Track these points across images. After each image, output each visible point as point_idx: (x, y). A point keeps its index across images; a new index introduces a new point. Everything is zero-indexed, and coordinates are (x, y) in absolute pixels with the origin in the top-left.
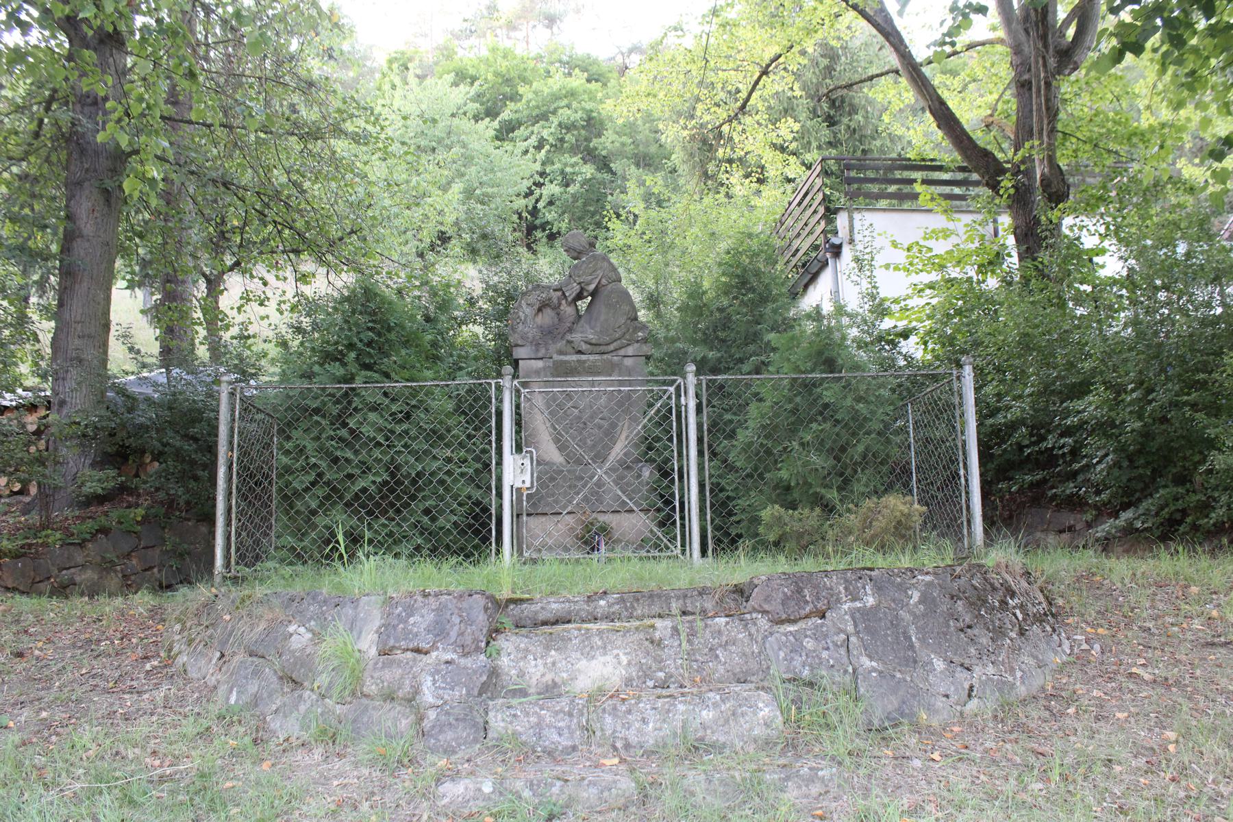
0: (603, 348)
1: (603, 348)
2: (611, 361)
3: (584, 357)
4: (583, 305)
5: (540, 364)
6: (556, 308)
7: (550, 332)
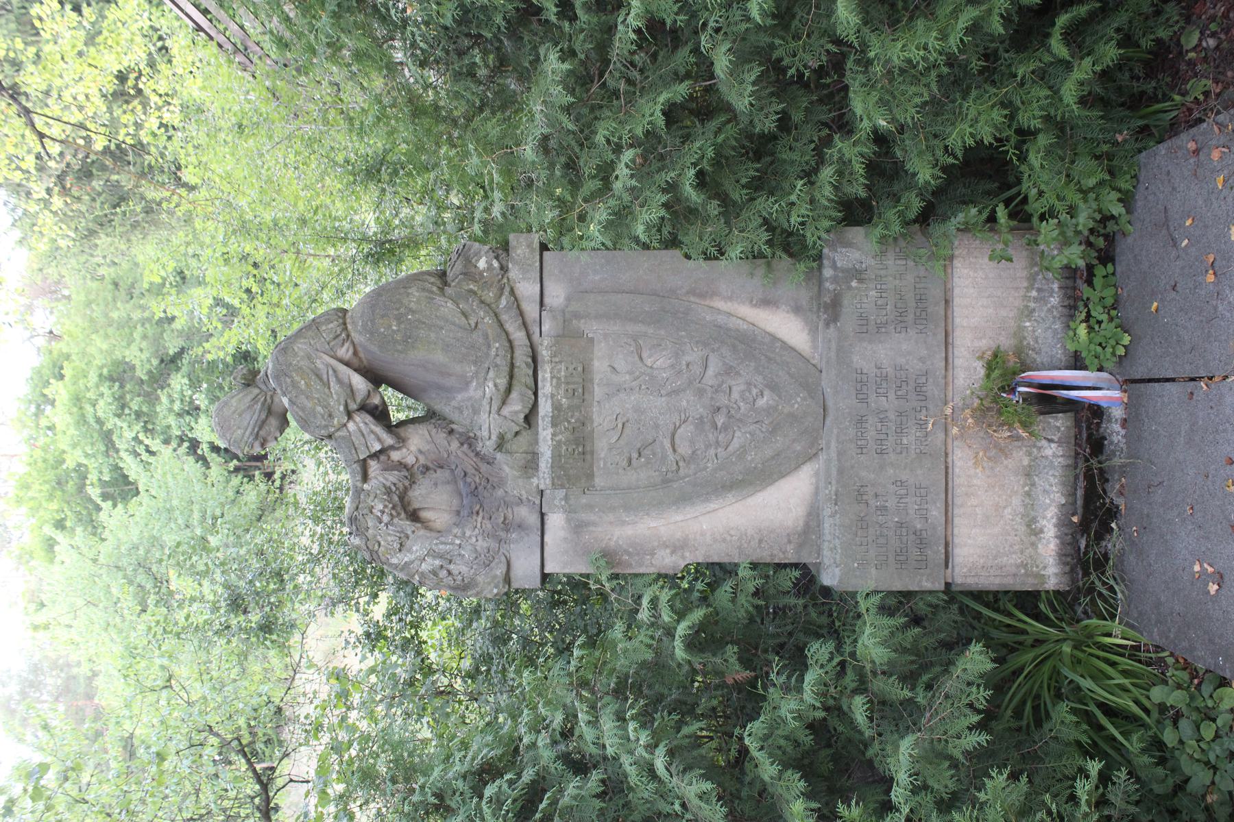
1: (522, 357)
3: (545, 408)
5: (556, 521)
7: (474, 493)
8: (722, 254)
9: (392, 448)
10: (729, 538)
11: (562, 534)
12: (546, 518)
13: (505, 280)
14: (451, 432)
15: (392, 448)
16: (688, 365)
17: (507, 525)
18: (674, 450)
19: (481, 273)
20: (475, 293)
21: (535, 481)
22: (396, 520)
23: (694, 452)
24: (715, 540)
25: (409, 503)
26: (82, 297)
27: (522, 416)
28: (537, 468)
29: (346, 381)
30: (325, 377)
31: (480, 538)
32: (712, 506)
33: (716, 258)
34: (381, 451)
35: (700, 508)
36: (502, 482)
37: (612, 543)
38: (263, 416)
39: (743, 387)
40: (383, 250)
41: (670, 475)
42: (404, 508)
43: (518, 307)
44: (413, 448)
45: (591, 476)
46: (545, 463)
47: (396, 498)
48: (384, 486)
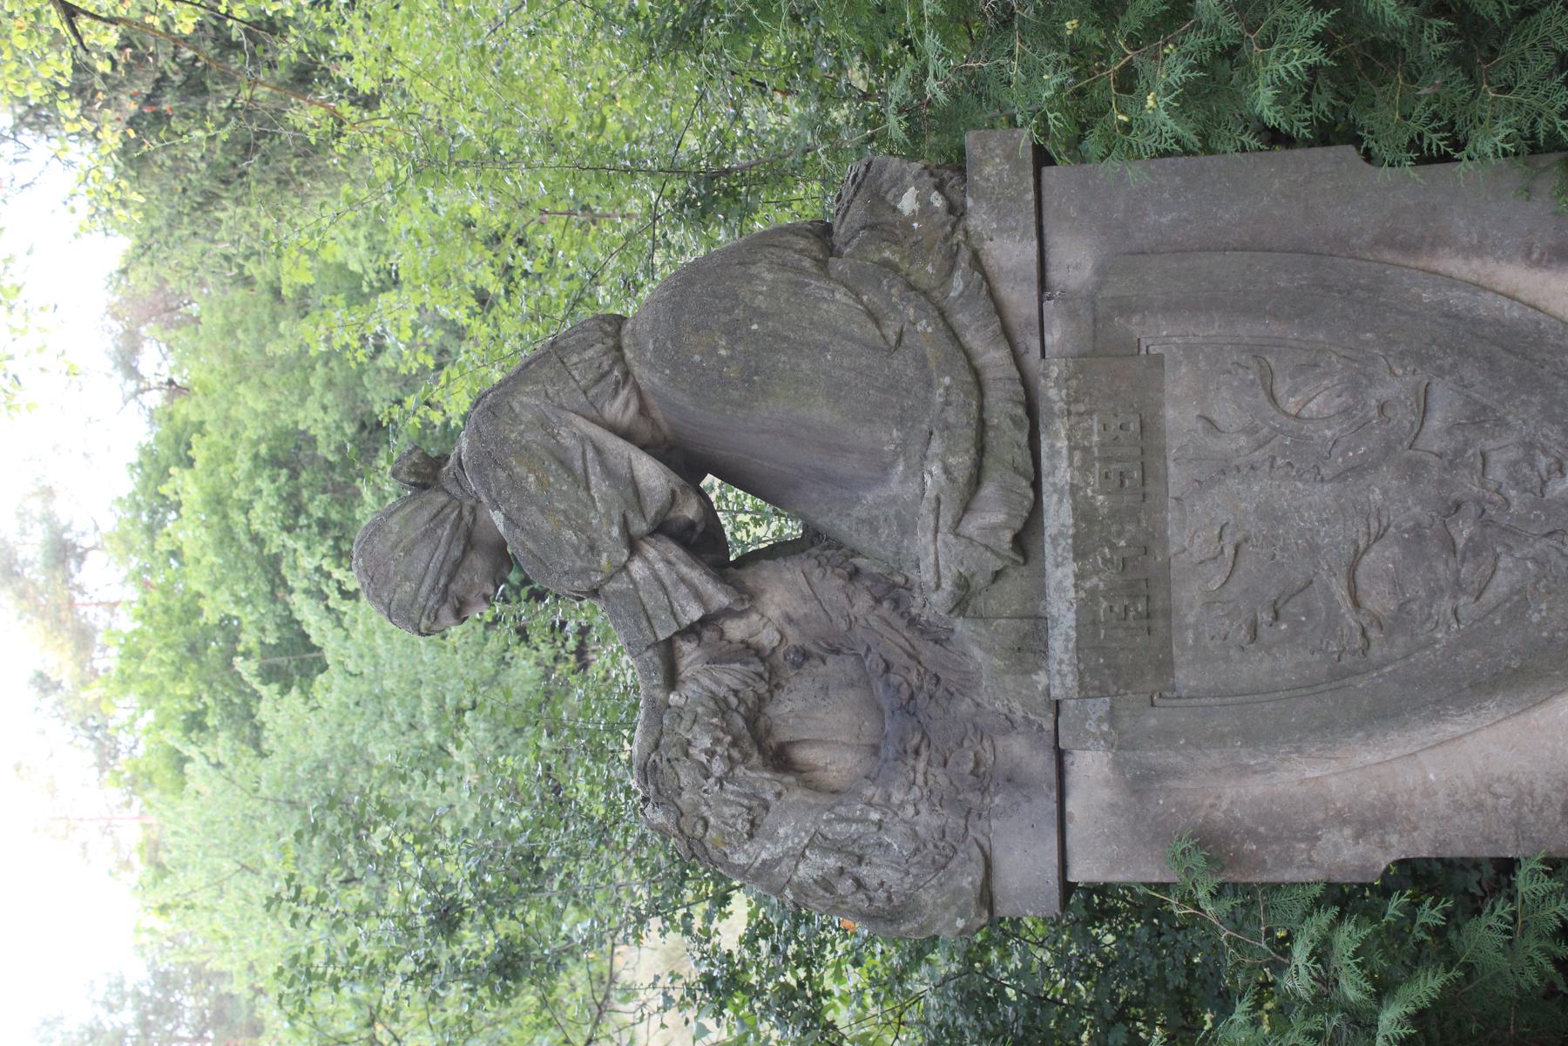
1: (1002, 406)
3: (1058, 516)
4: (749, 524)
5: (1090, 768)
7: (908, 708)
8: (1459, 146)
9: (728, 613)
10: (1490, 801)
11: (1105, 795)
12: (1068, 759)
13: (960, 236)
14: (855, 574)
15: (728, 613)
16: (1382, 408)
17: (981, 779)
18: (1356, 604)
19: (906, 224)
20: (895, 269)
21: (1041, 679)
22: (740, 771)
23: (1401, 607)
24: (1458, 807)
25: (768, 731)
26: (219, 319)
27: (1008, 536)
28: (1044, 652)
29: (624, 471)
30: (578, 464)
31: (923, 807)
32: (1450, 729)
33: (1446, 158)
34: (703, 621)
35: (1423, 734)
36: (968, 682)
37: (1219, 815)
38: (456, 553)
39: (1513, 454)
40: (712, 191)
41: (1347, 660)
42: (758, 742)
43: (991, 293)
44: (773, 612)
45: (1166, 666)
46: (1061, 640)
47: (739, 722)
48: (714, 696)
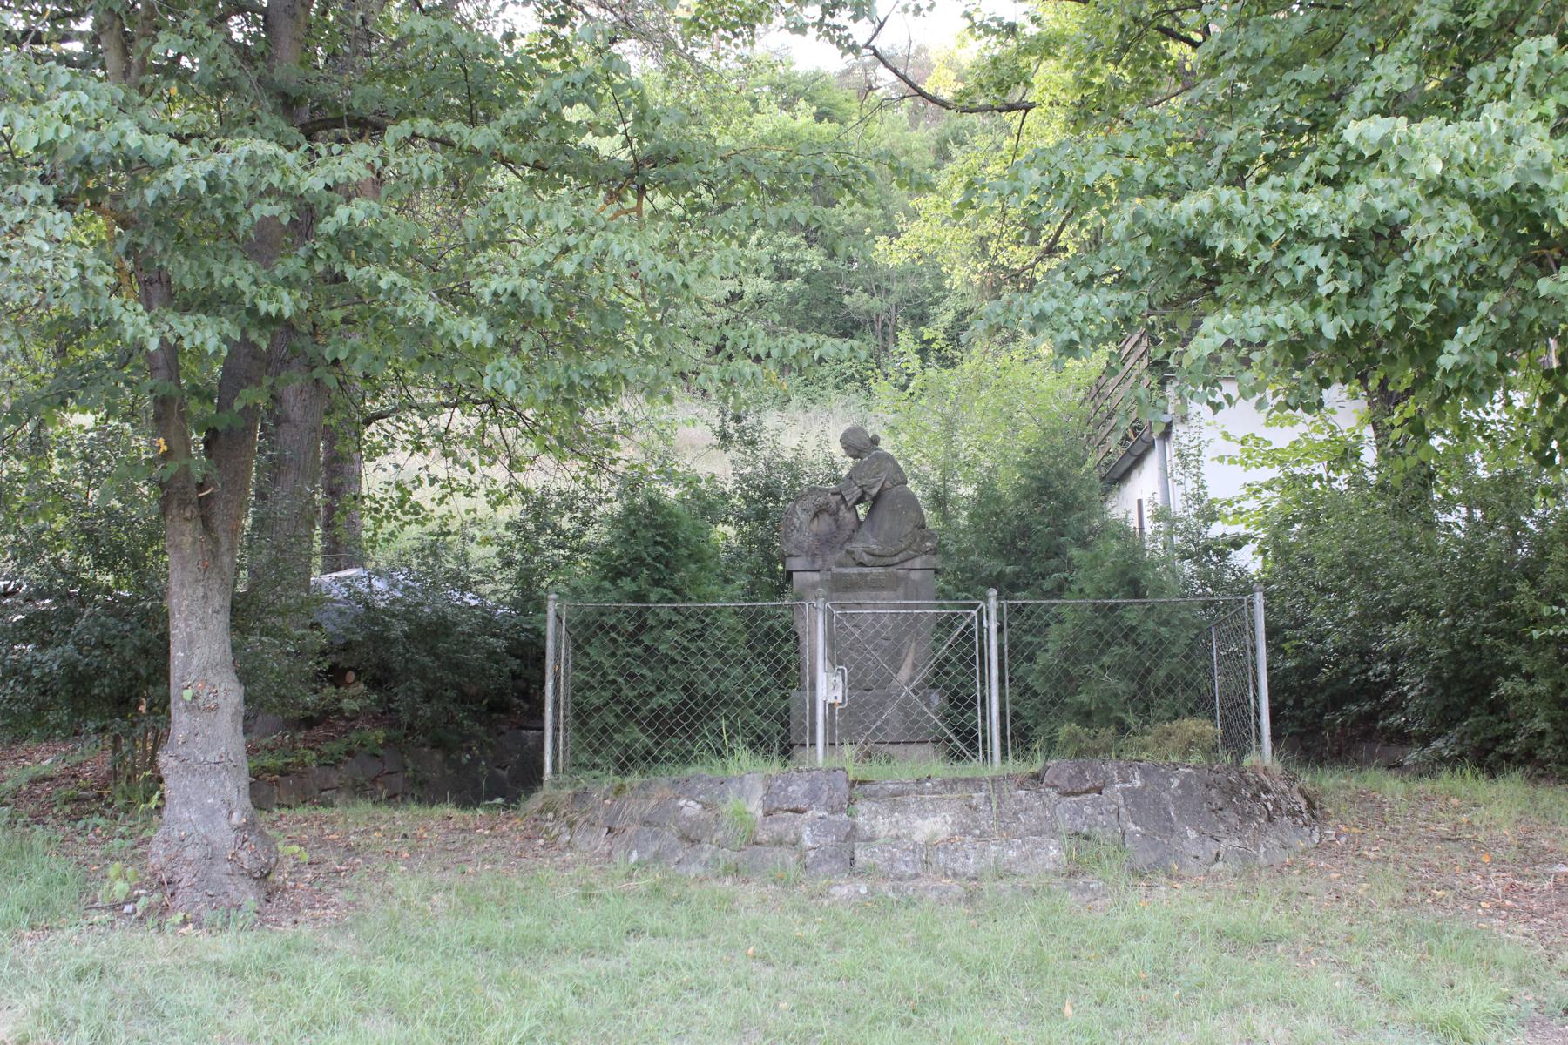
0: (887, 560)
1: (887, 560)
2: (896, 575)
3: (866, 570)
5: (816, 577)
6: (834, 514)
17: (814, 555)
26: (916, 145)
40: (940, 500)
